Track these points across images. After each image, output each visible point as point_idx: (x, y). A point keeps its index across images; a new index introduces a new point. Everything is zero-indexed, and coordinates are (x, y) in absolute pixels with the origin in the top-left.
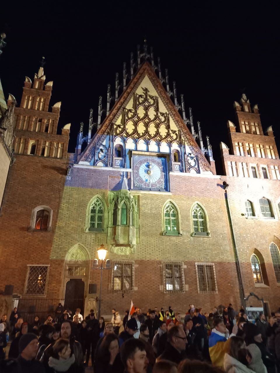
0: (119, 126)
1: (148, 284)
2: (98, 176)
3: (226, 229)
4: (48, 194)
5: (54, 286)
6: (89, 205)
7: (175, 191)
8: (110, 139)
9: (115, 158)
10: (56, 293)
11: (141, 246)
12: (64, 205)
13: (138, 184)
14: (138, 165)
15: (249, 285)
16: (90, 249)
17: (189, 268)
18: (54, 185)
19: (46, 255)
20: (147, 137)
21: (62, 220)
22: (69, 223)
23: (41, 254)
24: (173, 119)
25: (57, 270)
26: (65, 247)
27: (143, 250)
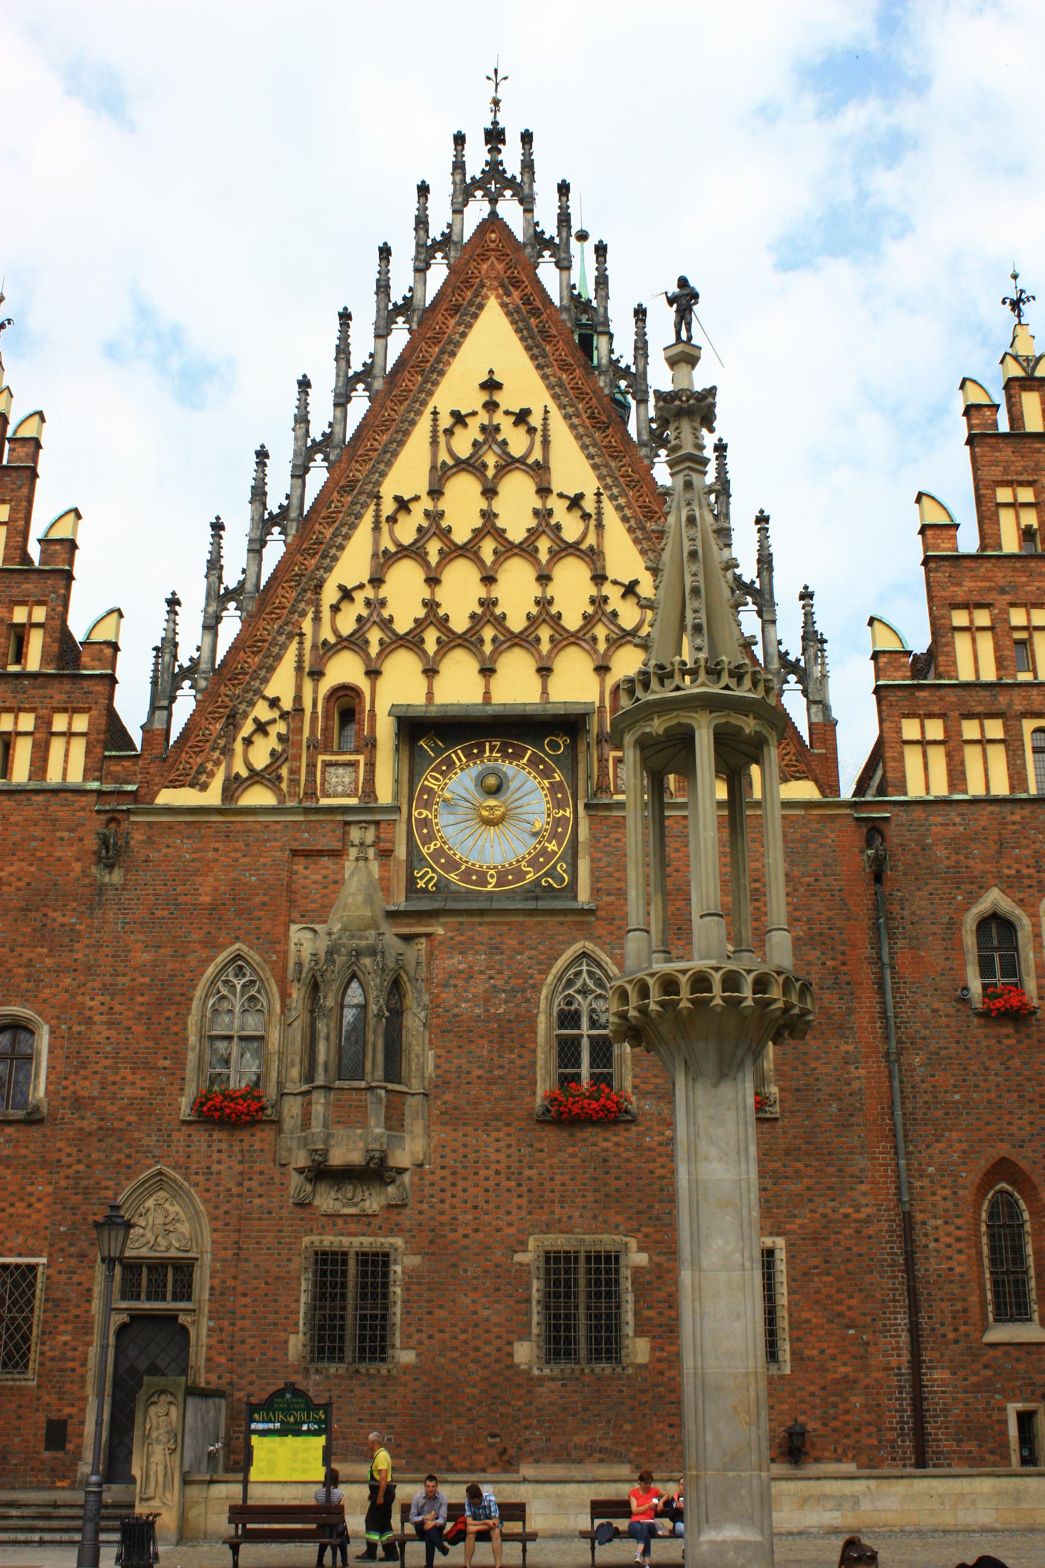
0: (346, 594)
1: (462, 1337)
2: (239, 855)
3: (862, 1072)
4: (26, 956)
5: (65, 1343)
6: (199, 992)
7: (612, 898)
8: (299, 668)
9: (321, 758)
10: (73, 1370)
11: (432, 1173)
12: (92, 999)
13: (431, 874)
14: (437, 779)
15: (951, 1335)
16: (207, 1190)
17: (659, 1265)
18: (51, 914)
19: (29, 1216)
20: (485, 636)
21: (85, 1068)
22: (118, 1078)
23: (11, 1215)
24: (625, 519)
25: (75, 1278)
26: (104, 1183)
27: (443, 1190)
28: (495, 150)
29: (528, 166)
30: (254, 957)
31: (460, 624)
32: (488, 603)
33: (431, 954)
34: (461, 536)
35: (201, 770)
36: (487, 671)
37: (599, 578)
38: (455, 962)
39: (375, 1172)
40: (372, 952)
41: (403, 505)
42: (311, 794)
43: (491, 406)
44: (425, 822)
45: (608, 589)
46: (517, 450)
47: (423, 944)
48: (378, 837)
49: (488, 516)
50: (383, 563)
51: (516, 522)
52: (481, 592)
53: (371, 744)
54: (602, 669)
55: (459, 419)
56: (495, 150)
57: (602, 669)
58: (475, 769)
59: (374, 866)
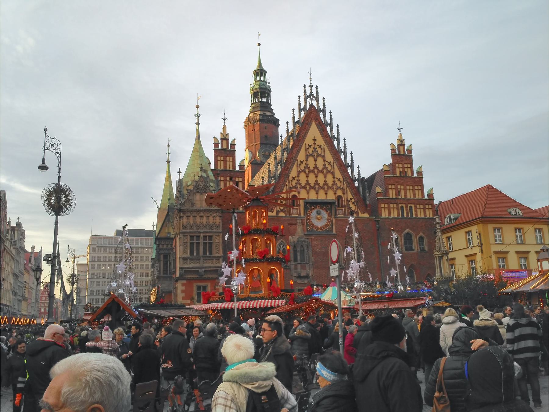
0: (294, 178)
20: (316, 187)
28: (311, 89)
29: (317, 93)
30: (284, 242)
31: (312, 185)
32: (316, 181)
33: (312, 241)
34: (311, 168)
35: (272, 209)
36: (317, 193)
37: (334, 177)
38: (316, 243)
39: (307, 277)
40: (305, 241)
41: (302, 162)
42: (290, 214)
43: (315, 144)
44: (309, 219)
45: (336, 180)
46: (319, 153)
47: (310, 240)
48: (302, 222)
49: (316, 165)
50: (299, 172)
51: (320, 167)
52: (315, 179)
53: (299, 205)
54: (335, 194)
55: (310, 146)
56: (311, 89)
57: (335, 194)
58: (316, 210)
59: (302, 226)
